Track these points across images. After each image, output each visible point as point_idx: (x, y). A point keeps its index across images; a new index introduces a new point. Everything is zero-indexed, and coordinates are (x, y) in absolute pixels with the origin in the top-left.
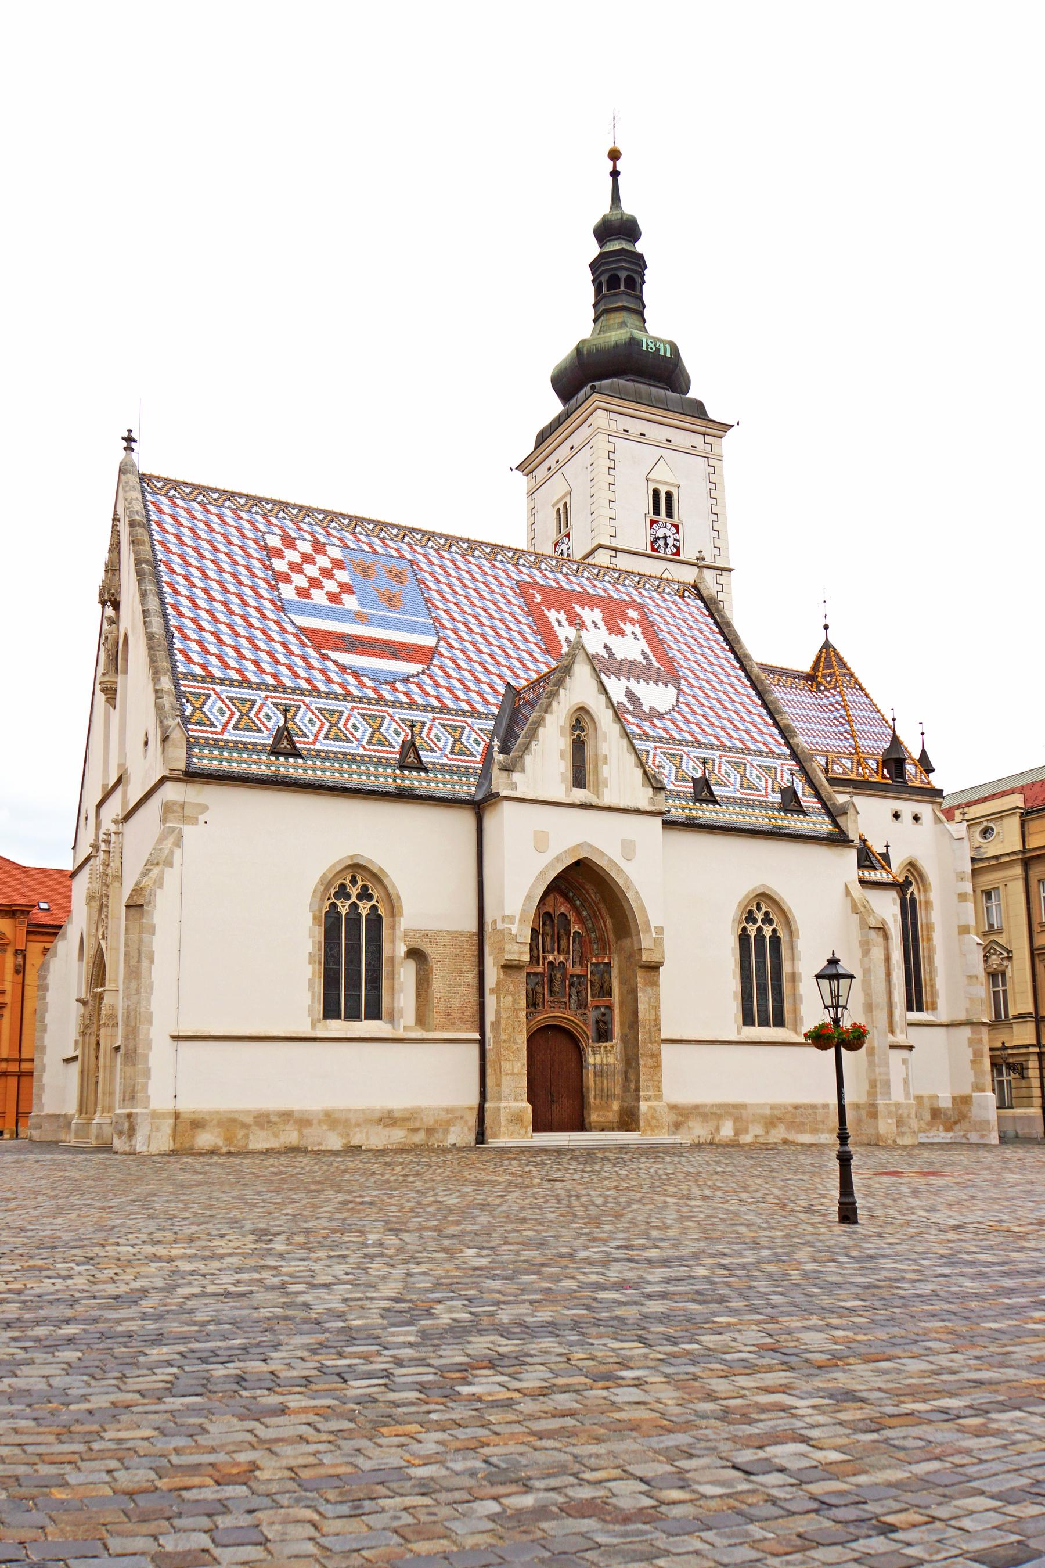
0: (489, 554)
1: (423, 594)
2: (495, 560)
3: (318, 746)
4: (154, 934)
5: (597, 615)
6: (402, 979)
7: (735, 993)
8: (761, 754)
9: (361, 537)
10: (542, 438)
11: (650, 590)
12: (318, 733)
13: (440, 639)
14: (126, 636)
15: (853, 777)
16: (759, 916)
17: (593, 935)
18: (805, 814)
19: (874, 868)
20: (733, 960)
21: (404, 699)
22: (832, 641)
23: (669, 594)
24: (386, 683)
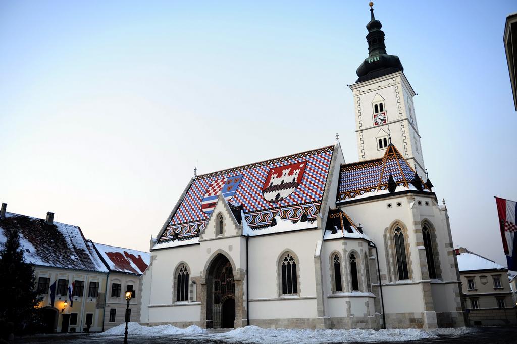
7: (277, 284)
16: (288, 258)
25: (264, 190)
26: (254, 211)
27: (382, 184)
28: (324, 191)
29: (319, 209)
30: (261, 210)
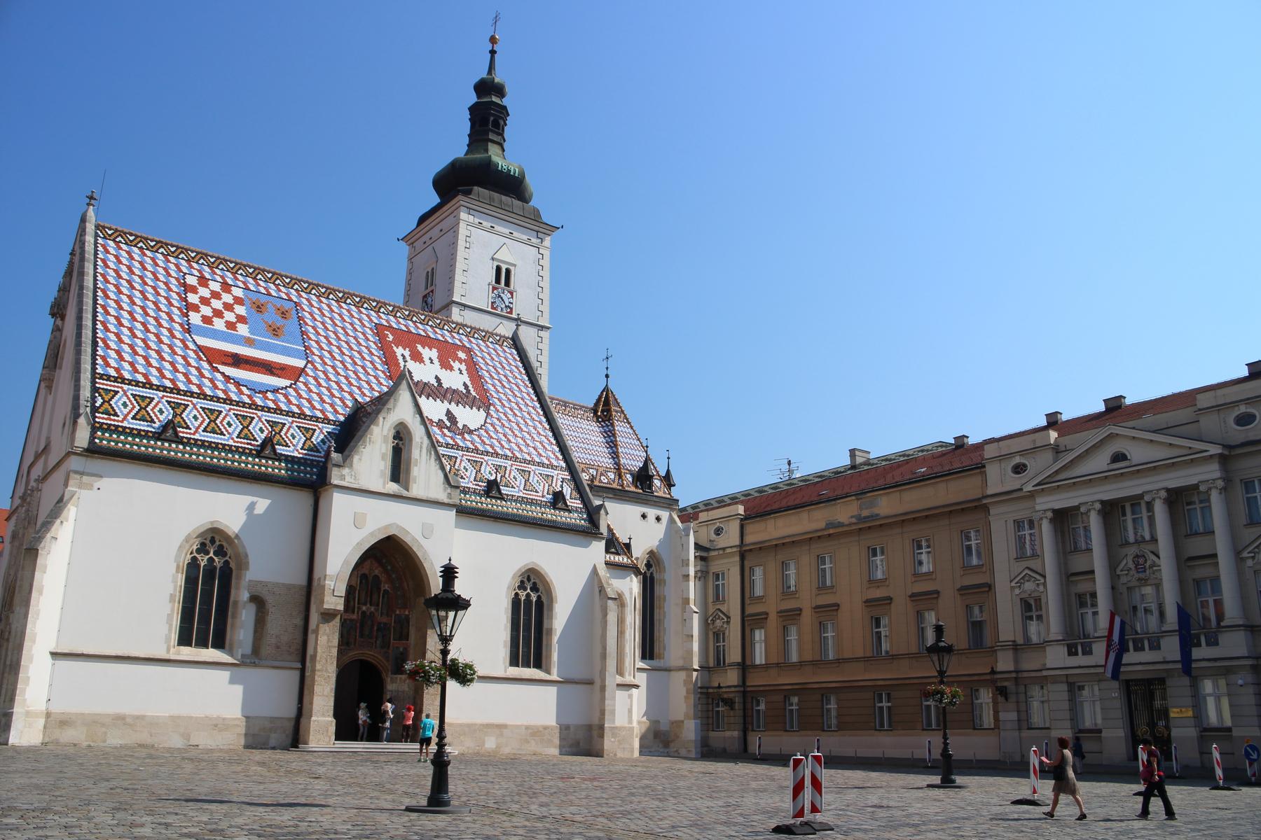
0: (358, 303)
1: (301, 327)
2: (362, 307)
3: (197, 436)
4: (45, 572)
5: (434, 353)
6: (243, 618)
7: (505, 642)
8: (543, 465)
9: (261, 283)
10: (423, 219)
11: (477, 338)
12: (200, 426)
13: (308, 362)
14: (65, 341)
15: (615, 486)
17: (399, 593)
18: (570, 511)
19: (618, 554)
20: (505, 617)
21: (272, 405)
22: (610, 386)
23: (492, 342)
24: (260, 392)
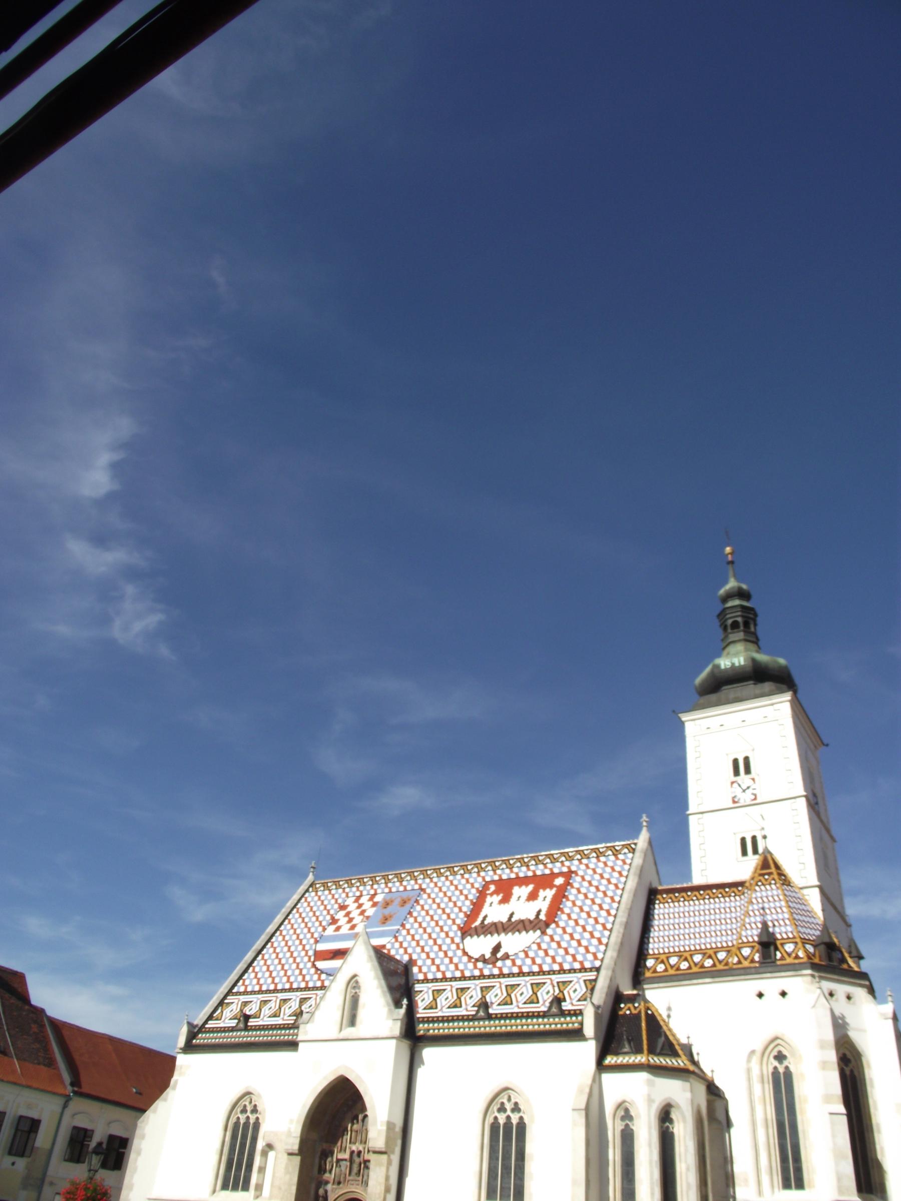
25: (466, 931)
26: (435, 980)
27: (743, 943)
28: (607, 945)
29: (592, 989)
30: (454, 979)
